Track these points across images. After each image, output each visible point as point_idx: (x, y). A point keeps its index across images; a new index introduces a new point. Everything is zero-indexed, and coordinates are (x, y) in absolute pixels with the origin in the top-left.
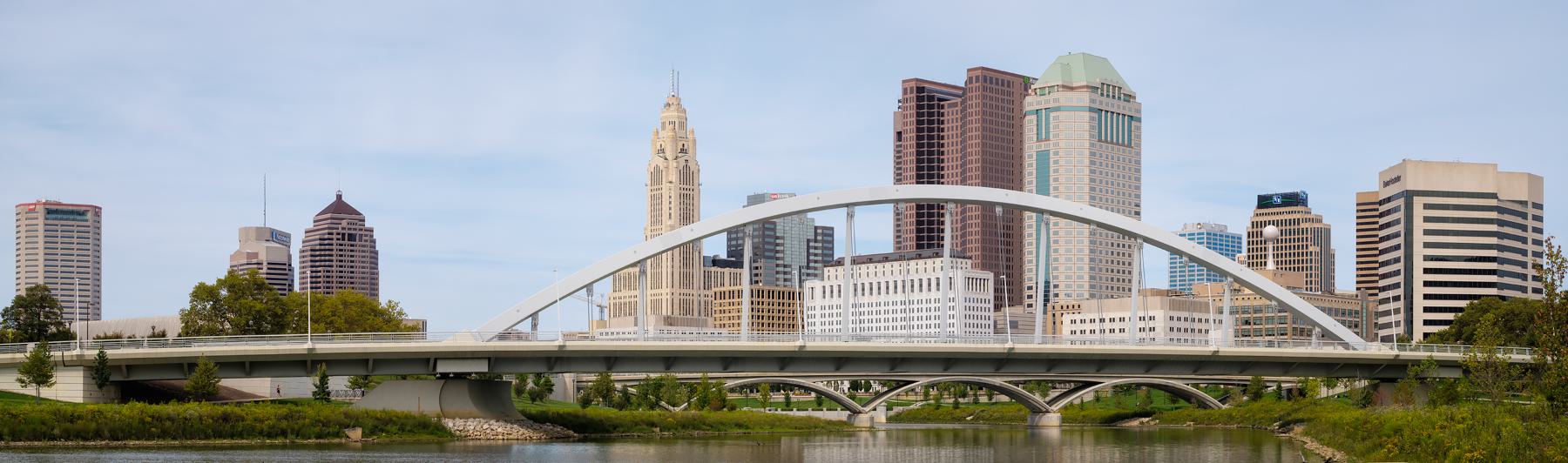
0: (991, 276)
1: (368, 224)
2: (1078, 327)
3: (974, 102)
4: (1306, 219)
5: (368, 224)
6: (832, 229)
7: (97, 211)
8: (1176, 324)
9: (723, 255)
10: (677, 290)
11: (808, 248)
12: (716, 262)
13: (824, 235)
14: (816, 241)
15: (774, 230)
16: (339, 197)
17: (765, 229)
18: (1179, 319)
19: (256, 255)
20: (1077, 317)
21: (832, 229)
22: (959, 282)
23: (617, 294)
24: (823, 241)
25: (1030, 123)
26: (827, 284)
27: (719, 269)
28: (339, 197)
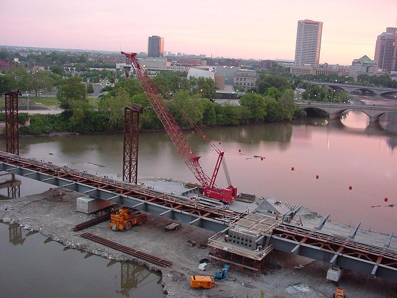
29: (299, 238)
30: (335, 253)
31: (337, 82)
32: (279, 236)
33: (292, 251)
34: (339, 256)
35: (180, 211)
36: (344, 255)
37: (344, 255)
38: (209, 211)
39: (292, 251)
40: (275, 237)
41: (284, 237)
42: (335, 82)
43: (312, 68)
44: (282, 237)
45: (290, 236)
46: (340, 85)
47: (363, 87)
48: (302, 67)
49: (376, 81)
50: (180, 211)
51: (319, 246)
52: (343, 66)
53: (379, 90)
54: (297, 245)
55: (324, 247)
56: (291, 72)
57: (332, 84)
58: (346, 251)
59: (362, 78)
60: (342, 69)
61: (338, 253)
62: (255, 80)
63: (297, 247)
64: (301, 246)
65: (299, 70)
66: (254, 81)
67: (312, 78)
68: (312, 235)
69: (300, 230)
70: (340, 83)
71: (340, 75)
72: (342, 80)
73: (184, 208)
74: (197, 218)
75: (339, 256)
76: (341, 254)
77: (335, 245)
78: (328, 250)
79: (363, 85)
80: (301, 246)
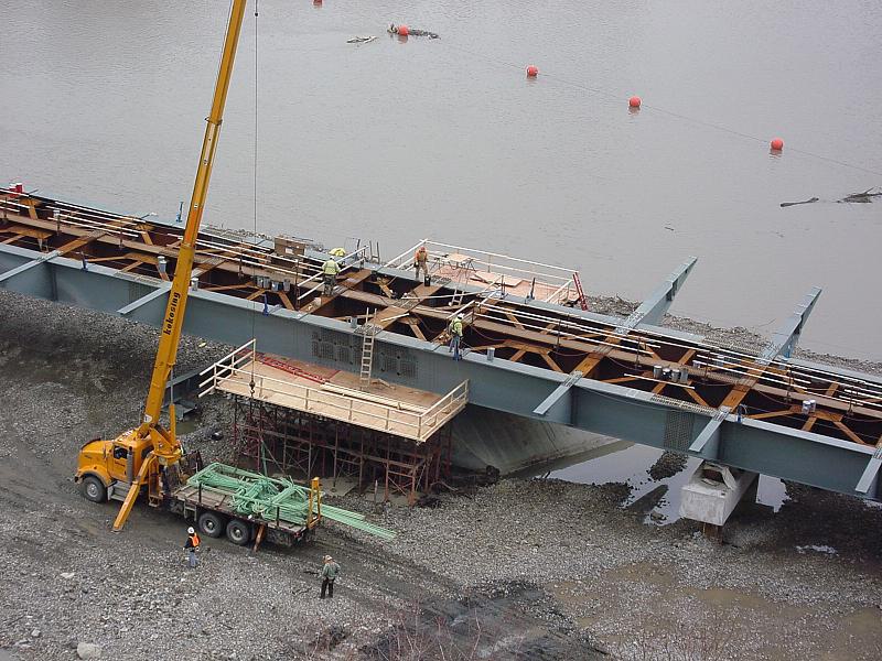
29: (568, 360)
30: (711, 411)
32: (485, 352)
33: (540, 410)
34: (725, 425)
35: (78, 264)
36: (748, 421)
37: (748, 421)
38: (203, 260)
39: (540, 410)
40: (470, 355)
41: (505, 354)
44: (498, 354)
45: (534, 349)
50: (76, 264)
51: (648, 386)
54: (559, 383)
55: (669, 391)
58: (755, 403)
61: (725, 412)
63: (561, 391)
64: (575, 391)
68: (622, 343)
69: (571, 325)
73: (97, 249)
74: (151, 289)
75: (725, 425)
76: (733, 418)
77: (712, 381)
78: (682, 404)
80: (575, 391)
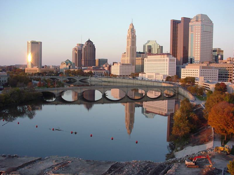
0: (176, 58)
1: (93, 44)
2: (184, 71)
3: (182, 23)
4: (215, 52)
5: (93, 44)
6: (162, 46)
7: (41, 43)
8: (202, 72)
9: (143, 52)
10: (131, 58)
11: (158, 50)
12: (140, 53)
13: (161, 48)
14: (159, 49)
15: (151, 47)
16: (89, 39)
17: (149, 47)
18: (203, 71)
19: (76, 49)
20: (184, 69)
21: (162, 46)
22: (168, 60)
23: (123, 58)
24: (161, 49)
25: (190, 27)
26: (148, 59)
27: (140, 54)
28: (89, 39)
31: (54, 76)
42: (53, 76)
43: (38, 69)
46: (56, 77)
47: (69, 77)
48: (33, 69)
49: (74, 73)
52: (56, 66)
53: (78, 78)
56: (26, 72)
57: (52, 77)
59: (68, 72)
60: (56, 68)
62: (7, 78)
65: (30, 70)
66: (6, 79)
67: (39, 74)
70: (56, 76)
71: (55, 71)
72: (57, 74)
79: (69, 76)
